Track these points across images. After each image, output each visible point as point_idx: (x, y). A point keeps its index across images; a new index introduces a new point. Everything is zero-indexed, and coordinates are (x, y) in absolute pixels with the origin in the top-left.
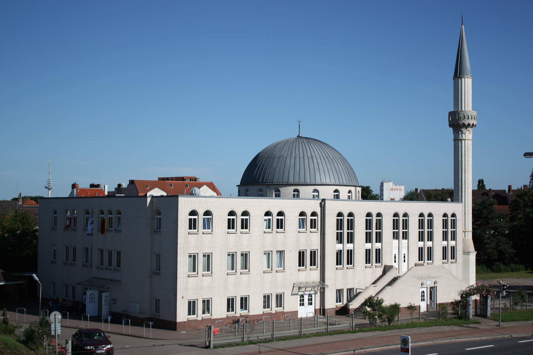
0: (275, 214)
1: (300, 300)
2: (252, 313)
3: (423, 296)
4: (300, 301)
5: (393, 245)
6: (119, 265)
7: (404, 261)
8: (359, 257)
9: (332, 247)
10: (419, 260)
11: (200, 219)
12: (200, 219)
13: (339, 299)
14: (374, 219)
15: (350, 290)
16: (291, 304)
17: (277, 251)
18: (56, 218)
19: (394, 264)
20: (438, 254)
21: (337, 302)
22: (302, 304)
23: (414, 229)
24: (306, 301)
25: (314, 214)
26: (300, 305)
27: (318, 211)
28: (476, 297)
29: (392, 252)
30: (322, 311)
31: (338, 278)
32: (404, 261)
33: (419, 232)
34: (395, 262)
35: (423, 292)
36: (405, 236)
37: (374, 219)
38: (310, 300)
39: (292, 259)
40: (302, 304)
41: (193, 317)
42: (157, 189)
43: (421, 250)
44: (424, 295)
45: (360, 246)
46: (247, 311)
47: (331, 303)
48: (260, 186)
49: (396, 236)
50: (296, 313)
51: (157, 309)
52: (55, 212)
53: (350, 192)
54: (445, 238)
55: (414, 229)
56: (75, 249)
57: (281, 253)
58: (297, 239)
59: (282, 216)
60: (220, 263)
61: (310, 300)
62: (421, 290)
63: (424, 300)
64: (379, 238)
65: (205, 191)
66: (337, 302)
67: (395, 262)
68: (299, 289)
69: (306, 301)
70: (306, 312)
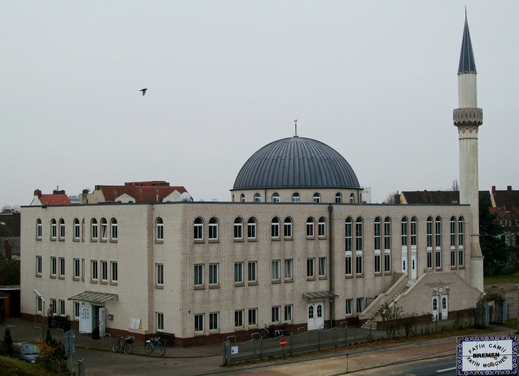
0: (282, 220)
1: (310, 311)
2: (261, 326)
3: (435, 304)
4: (310, 313)
5: (403, 251)
6: (115, 277)
7: (413, 268)
8: (369, 266)
9: (341, 254)
10: (428, 267)
11: (205, 227)
12: (205, 227)
13: (348, 310)
14: (383, 223)
15: (359, 300)
16: (298, 317)
17: (285, 260)
18: (40, 228)
19: (403, 271)
20: (446, 259)
21: (347, 313)
22: (311, 316)
23: (422, 235)
24: (315, 313)
25: (322, 219)
26: (310, 317)
27: (326, 216)
28: (491, 304)
29: (401, 258)
30: (330, 323)
31: (345, 288)
32: (413, 268)
33: (428, 236)
34: (404, 269)
35: (435, 300)
36: (414, 241)
37: (457, 222)
38: (319, 311)
39: (299, 268)
40: (311, 316)
41: (200, 333)
42: (125, 195)
43: (429, 255)
44: (436, 303)
45: (369, 252)
46: (254, 325)
47: (340, 314)
48: (257, 191)
49: (404, 242)
50: (306, 325)
51: (161, 324)
52: (39, 221)
53: (352, 195)
54: (453, 243)
55: (422, 235)
56: (63, 261)
57: (288, 262)
58: (301, 247)
59: (290, 222)
60: (225, 274)
61: (319, 311)
62: (433, 298)
63: (436, 309)
64: (387, 245)
65: (176, 196)
66: (347, 313)
67: (404, 269)
68: (308, 298)
69: (315, 313)
70: (316, 324)
